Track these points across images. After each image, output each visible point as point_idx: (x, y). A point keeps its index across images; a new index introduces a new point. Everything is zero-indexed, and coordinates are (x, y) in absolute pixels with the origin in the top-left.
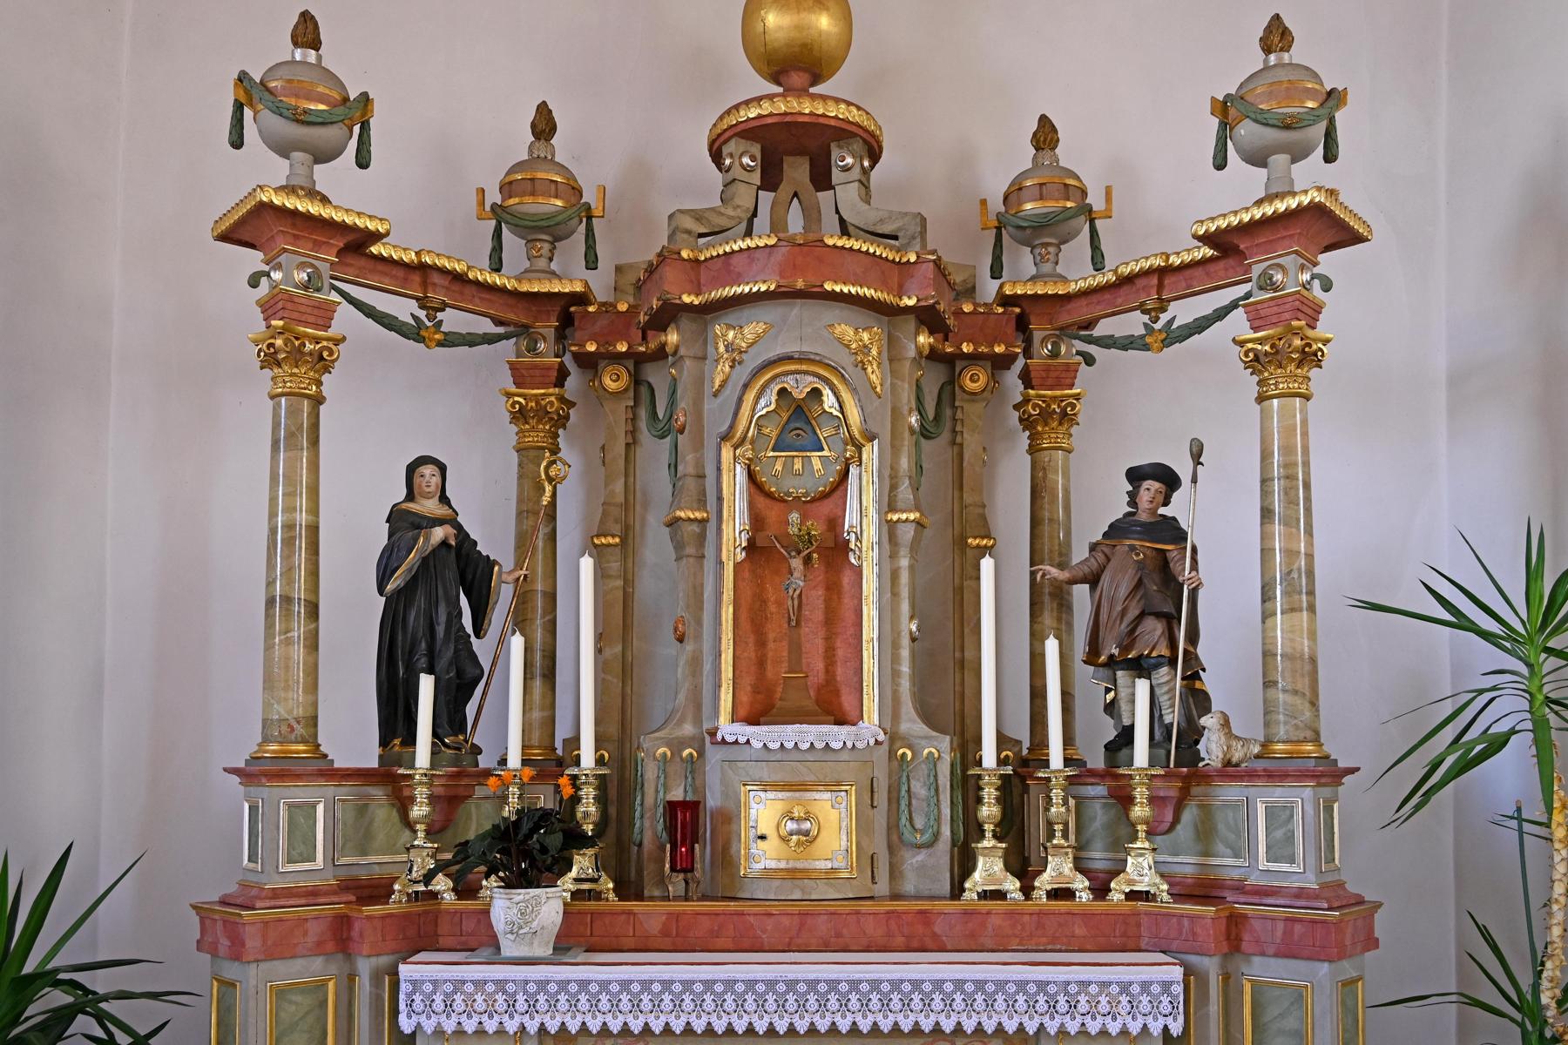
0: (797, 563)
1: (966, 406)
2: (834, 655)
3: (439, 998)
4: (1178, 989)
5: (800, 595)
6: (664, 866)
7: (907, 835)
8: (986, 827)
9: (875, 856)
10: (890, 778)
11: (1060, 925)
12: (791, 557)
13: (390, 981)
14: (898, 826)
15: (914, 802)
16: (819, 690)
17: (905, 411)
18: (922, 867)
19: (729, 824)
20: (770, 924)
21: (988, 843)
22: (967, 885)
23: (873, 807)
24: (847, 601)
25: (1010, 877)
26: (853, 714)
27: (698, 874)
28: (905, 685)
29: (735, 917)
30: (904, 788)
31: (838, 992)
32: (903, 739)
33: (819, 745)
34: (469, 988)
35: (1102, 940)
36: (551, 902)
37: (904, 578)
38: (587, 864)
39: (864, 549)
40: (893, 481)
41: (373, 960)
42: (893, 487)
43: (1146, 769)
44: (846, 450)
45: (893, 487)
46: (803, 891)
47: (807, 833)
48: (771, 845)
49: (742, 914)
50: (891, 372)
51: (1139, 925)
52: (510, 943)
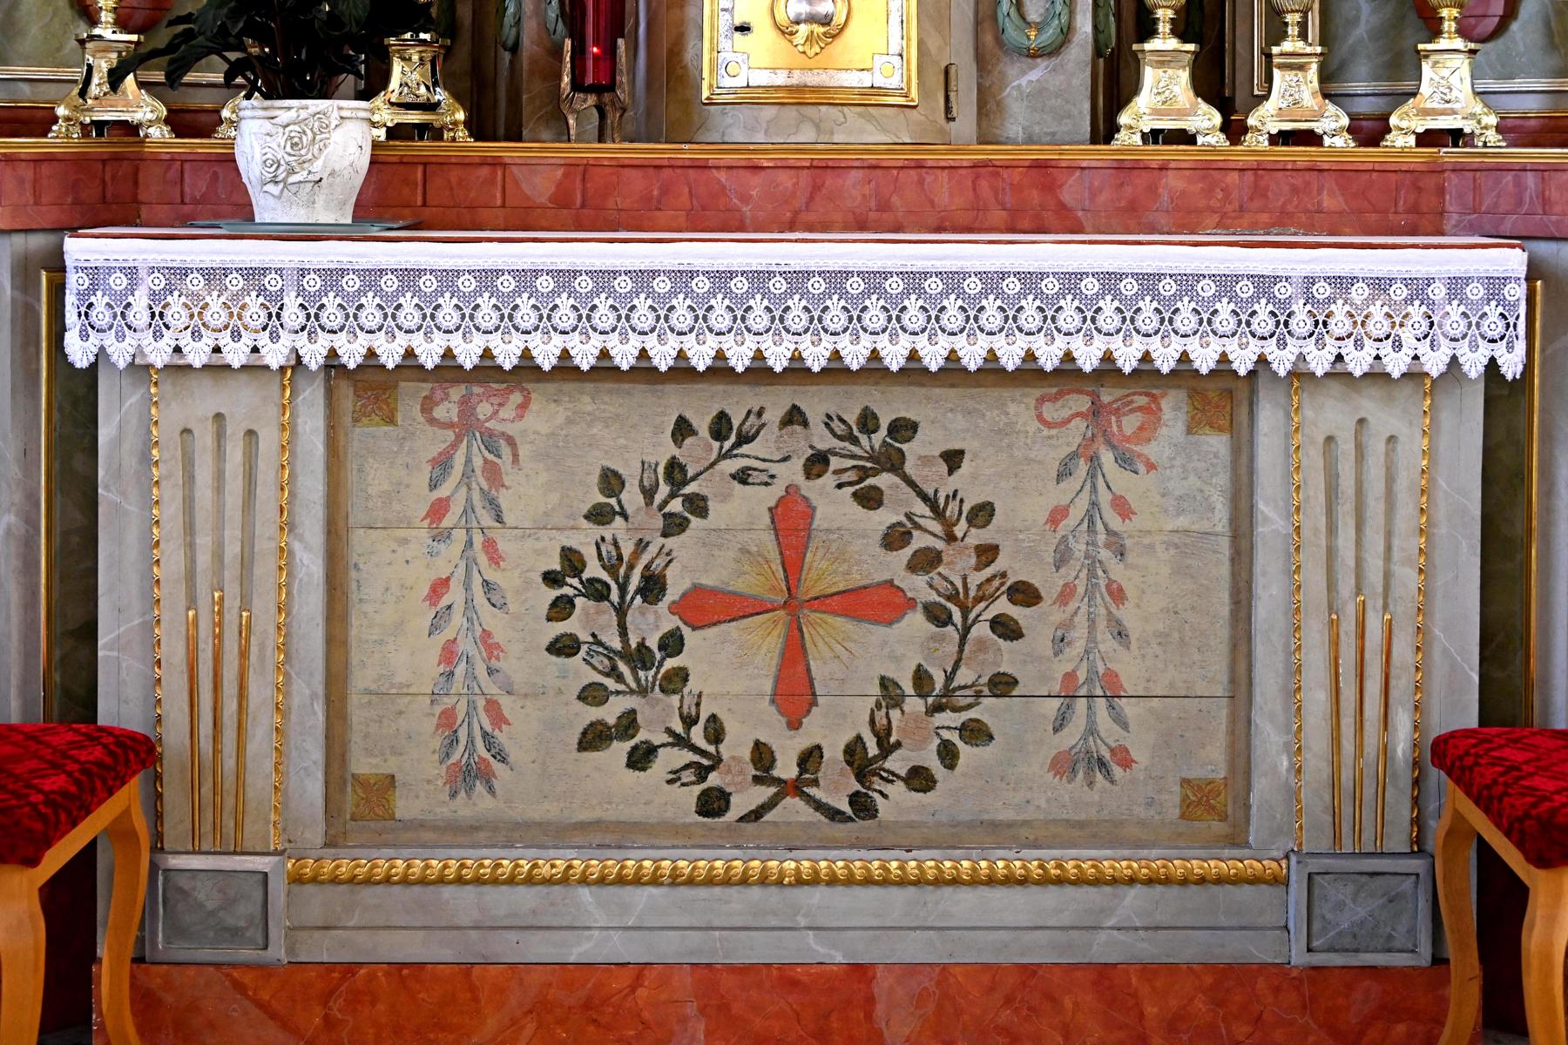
3: (140, 301)
4: (1517, 292)
6: (560, 78)
7: (1012, 33)
8: (1160, 13)
9: (953, 70)
11: (1295, 190)
13: (49, 281)
14: (994, 18)
18: (1039, 93)
19: (682, 7)
20: (755, 185)
21: (1164, 42)
22: (1124, 119)
25: (1204, 107)
27: (622, 94)
29: (691, 171)
31: (884, 295)
34: (196, 283)
35: (1374, 217)
36: (349, 125)
38: (416, 76)
41: (18, 240)
46: (817, 127)
47: (826, 21)
48: (764, 39)
49: (703, 166)
51: (1441, 191)
52: (271, 201)
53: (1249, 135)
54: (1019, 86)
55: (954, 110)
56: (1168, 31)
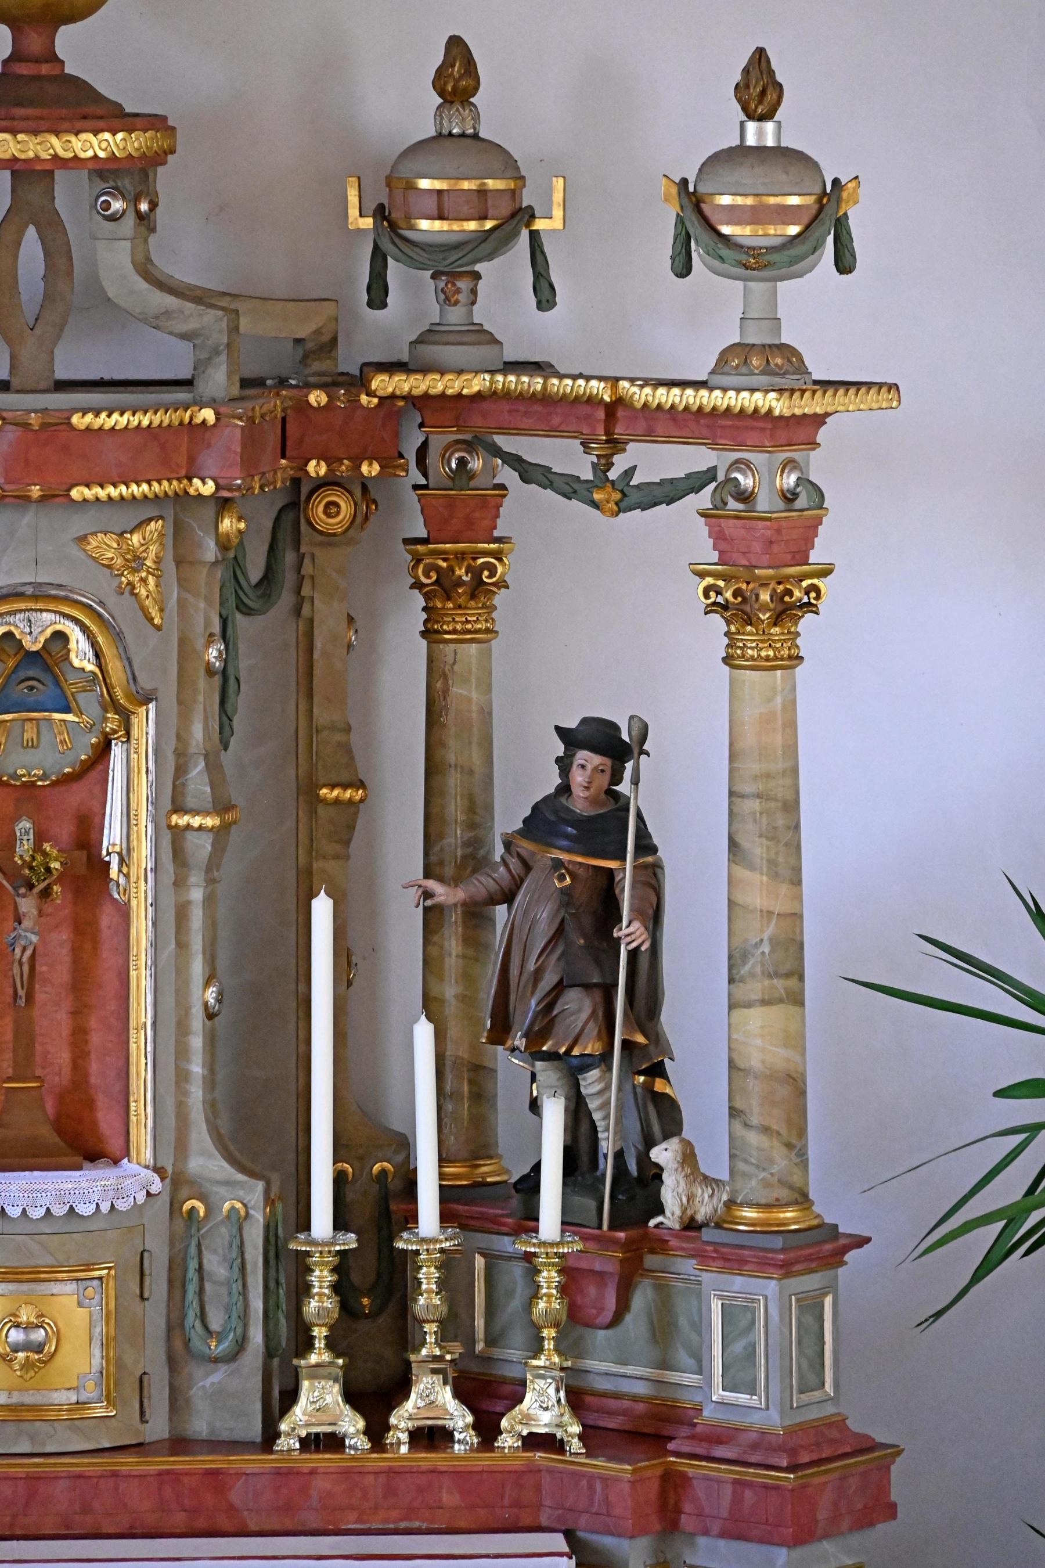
0: (27, 905)
1: (318, 552)
2: (86, 1042)
5: (33, 957)
8: (316, 1332)
10: (172, 1243)
12: (18, 895)
15: (208, 1287)
16: (61, 1098)
17: (200, 642)
18: (218, 1395)
23: (142, 1297)
24: (107, 955)
26: (114, 1145)
28: (196, 1093)
30: (193, 1265)
32: (192, 1183)
33: (59, 1211)
37: (197, 918)
39: (133, 879)
40: (181, 761)
42: (181, 771)
43: (557, 1244)
44: (105, 719)
45: (181, 771)
50: (179, 580)
53: (391, 1433)
54: (204, 1387)
55: (147, 1414)
56: (322, 1346)
